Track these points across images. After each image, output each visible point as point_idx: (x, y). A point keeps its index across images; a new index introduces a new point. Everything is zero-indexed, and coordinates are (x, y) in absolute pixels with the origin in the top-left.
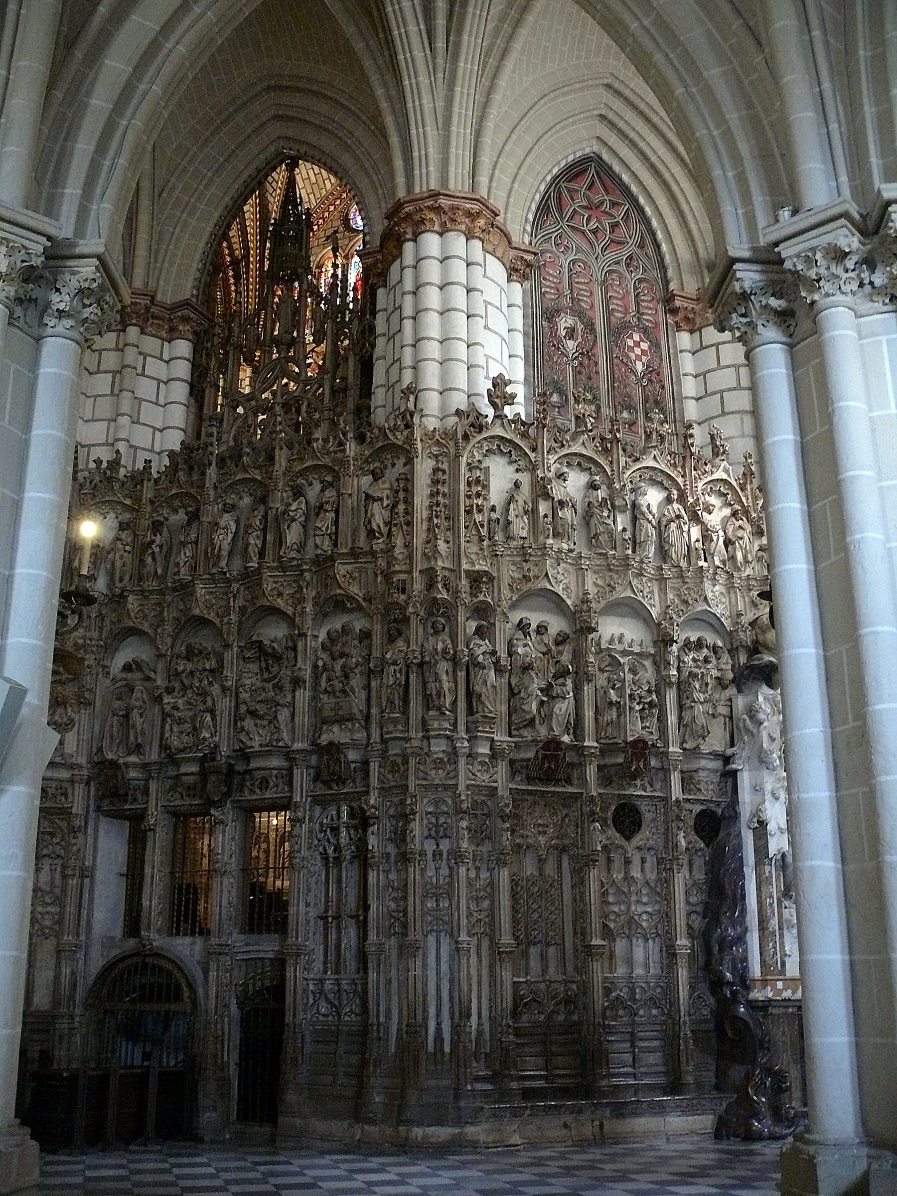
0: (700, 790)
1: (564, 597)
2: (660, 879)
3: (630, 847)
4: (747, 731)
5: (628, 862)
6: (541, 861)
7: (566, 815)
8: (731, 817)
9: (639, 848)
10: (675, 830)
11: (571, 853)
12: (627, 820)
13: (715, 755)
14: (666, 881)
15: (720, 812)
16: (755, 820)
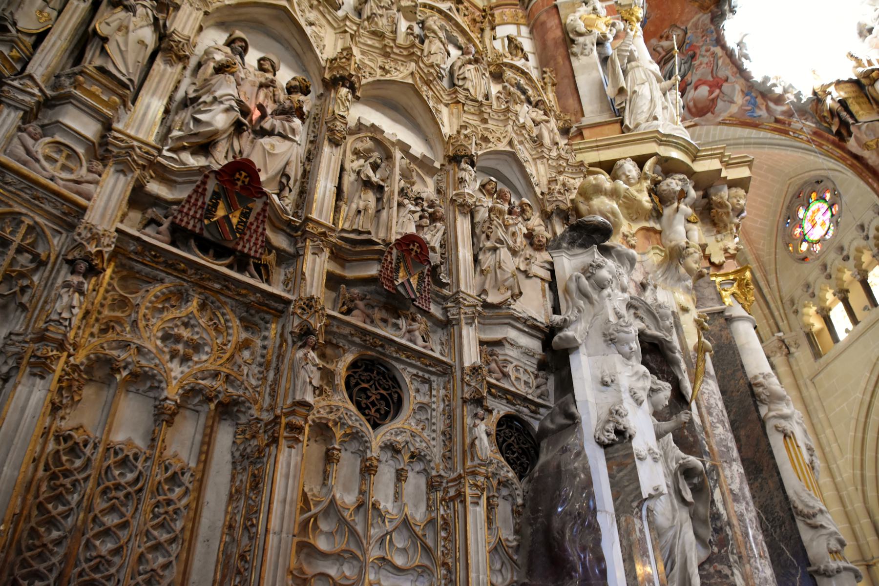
0: (506, 375)
1: (315, 45)
2: (432, 522)
3: (377, 438)
4: (585, 295)
5: (368, 470)
6: (164, 416)
7: (246, 345)
8: (562, 428)
9: (393, 449)
10: (468, 421)
11: (243, 419)
12: (376, 387)
13: (531, 327)
14: (446, 525)
15: (536, 425)
16: (611, 426)
